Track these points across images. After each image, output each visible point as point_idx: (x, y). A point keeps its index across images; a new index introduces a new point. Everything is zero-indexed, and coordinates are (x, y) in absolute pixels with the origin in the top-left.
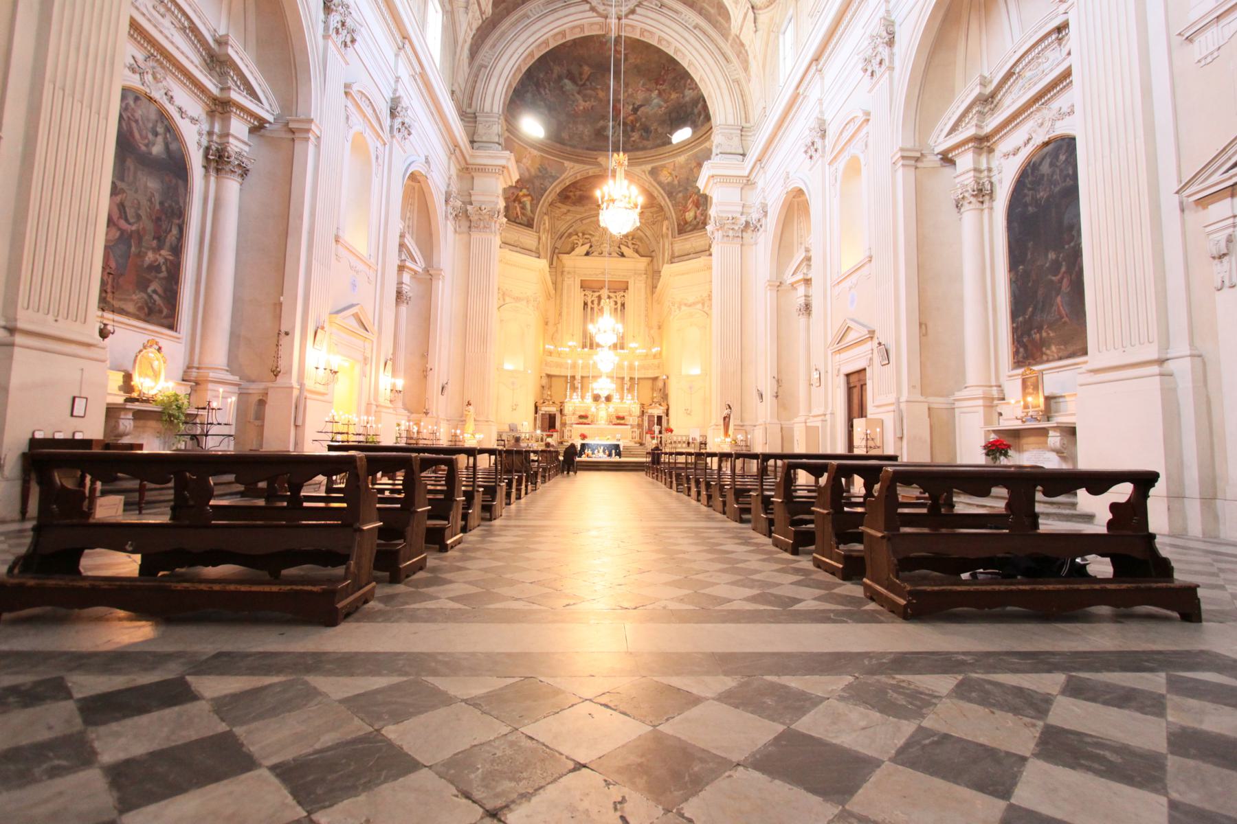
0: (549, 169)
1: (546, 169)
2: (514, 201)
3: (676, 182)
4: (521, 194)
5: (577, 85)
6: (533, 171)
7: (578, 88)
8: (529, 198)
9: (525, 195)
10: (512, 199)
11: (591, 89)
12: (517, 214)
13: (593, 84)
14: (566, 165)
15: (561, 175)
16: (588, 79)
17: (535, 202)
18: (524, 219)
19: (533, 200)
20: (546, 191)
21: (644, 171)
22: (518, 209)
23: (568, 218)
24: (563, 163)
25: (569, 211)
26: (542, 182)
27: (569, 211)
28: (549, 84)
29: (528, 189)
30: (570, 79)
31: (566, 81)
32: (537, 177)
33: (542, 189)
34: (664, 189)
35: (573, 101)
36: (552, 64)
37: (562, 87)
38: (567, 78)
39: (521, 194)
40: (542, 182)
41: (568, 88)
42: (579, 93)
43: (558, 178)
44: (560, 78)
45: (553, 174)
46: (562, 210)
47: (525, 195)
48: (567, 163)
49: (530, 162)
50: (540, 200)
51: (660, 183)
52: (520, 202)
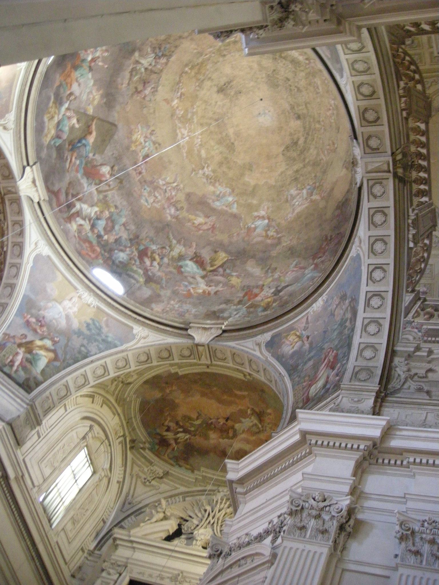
0: (105, 330)
1: (100, 329)
2: (20, 345)
3: (307, 346)
4: (39, 343)
5: (204, 269)
6: (76, 325)
7: (203, 273)
8: (51, 355)
9: (44, 348)
10: (18, 341)
11: (223, 275)
12: (12, 362)
13: (228, 271)
14: (135, 332)
15: (122, 345)
16: (222, 266)
17: (57, 364)
18: (22, 373)
19: (56, 359)
20: (85, 357)
21: (259, 345)
22: (19, 358)
23: (164, 487)
24: (132, 328)
25: (167, 474)
26: (85, 342)
27: (167, 474)
28: (162, 259)
29: (55, 343)
30: (196, 262)
31: (190, 263)
32: (79, 333)
33: (80, 352)
34: (283, 364)
35: (190, 283)
36: (174, 242)
37: (181, 267)
38: (191, 260)
39: (39, 343)
40: (85, 342)
41: (188, 269)
42: (203, 277)
43: (116, 346)
44: (181, 257)
45: (110, 339)
46: (155, 468)
47: (44, 348)
48: (138, 329)
49: (75, 309)
50: (70, 365)
51: (279, 358)
52: (29, 351)
